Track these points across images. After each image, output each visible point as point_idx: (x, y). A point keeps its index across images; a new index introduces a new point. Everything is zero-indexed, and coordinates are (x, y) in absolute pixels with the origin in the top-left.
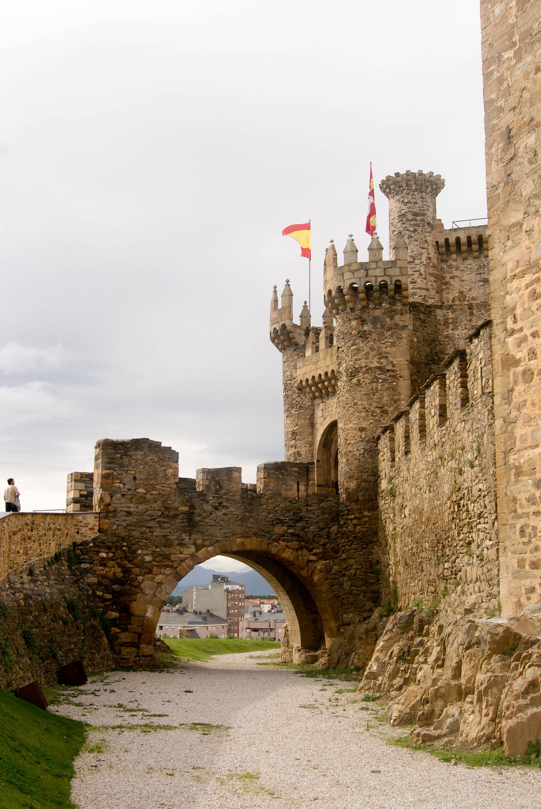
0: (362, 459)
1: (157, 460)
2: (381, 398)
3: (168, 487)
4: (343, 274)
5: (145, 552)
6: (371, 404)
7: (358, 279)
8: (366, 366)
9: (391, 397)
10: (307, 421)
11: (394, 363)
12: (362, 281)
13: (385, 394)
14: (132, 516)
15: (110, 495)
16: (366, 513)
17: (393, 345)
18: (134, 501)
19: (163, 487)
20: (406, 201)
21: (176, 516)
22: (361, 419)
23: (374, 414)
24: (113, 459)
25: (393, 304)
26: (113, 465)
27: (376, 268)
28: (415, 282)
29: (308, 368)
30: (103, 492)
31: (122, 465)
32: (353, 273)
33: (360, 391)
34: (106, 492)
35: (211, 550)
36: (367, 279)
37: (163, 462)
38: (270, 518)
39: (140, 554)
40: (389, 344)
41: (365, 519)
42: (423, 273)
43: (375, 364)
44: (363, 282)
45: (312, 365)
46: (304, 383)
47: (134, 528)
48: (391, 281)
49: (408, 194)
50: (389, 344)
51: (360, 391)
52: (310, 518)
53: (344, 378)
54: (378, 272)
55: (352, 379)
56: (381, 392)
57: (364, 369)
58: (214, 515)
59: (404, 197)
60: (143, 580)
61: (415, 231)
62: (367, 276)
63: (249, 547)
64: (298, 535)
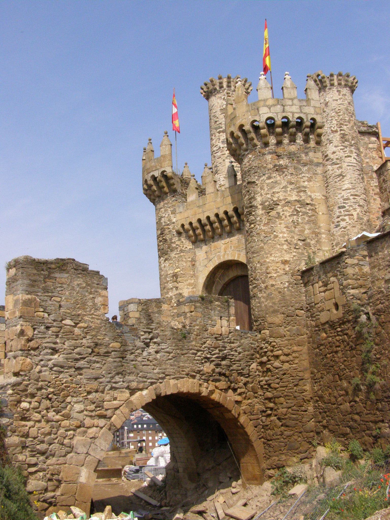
1: (84, 285)
2: (303, 231)
3: (98, 319)
4: (258, 109)
5: (75, 399)
6: (293, 237)
10: (189, 264)
11: (312, 197)
13: (307, 227)
15: (32, 327)
16: (295, 348)
17: (309, 180)
18: (60, 336)
19: (92, 318)
21: (107, 354)
22: (284, 252)
23: (297, 247)
26: (36, 289)
27: (292, 105)
29: (189, 213)
30: (25, 323)
32: (270, 108)
34: (28, 323)
35: (146, 395)
36: (284, 115)
38: (199, 356)
39: (70, 403)
40: (307, 178)
41: (294, 355)
43: (294, 198)
44: (280, 117)
45: (196, 209)
46: (187, 226)
47: (62, 370)
48: (307, 118)
50: (307, 178)
51: (280, 224)
52: (233, 355)
53: (260, 212)
54: (295, 109)
56: (302, 225)
57: (283, 202)
58: (145, 354)
59: (225, 95)
60: (74, 435)
62: (284, 111)
64: (224, 375)
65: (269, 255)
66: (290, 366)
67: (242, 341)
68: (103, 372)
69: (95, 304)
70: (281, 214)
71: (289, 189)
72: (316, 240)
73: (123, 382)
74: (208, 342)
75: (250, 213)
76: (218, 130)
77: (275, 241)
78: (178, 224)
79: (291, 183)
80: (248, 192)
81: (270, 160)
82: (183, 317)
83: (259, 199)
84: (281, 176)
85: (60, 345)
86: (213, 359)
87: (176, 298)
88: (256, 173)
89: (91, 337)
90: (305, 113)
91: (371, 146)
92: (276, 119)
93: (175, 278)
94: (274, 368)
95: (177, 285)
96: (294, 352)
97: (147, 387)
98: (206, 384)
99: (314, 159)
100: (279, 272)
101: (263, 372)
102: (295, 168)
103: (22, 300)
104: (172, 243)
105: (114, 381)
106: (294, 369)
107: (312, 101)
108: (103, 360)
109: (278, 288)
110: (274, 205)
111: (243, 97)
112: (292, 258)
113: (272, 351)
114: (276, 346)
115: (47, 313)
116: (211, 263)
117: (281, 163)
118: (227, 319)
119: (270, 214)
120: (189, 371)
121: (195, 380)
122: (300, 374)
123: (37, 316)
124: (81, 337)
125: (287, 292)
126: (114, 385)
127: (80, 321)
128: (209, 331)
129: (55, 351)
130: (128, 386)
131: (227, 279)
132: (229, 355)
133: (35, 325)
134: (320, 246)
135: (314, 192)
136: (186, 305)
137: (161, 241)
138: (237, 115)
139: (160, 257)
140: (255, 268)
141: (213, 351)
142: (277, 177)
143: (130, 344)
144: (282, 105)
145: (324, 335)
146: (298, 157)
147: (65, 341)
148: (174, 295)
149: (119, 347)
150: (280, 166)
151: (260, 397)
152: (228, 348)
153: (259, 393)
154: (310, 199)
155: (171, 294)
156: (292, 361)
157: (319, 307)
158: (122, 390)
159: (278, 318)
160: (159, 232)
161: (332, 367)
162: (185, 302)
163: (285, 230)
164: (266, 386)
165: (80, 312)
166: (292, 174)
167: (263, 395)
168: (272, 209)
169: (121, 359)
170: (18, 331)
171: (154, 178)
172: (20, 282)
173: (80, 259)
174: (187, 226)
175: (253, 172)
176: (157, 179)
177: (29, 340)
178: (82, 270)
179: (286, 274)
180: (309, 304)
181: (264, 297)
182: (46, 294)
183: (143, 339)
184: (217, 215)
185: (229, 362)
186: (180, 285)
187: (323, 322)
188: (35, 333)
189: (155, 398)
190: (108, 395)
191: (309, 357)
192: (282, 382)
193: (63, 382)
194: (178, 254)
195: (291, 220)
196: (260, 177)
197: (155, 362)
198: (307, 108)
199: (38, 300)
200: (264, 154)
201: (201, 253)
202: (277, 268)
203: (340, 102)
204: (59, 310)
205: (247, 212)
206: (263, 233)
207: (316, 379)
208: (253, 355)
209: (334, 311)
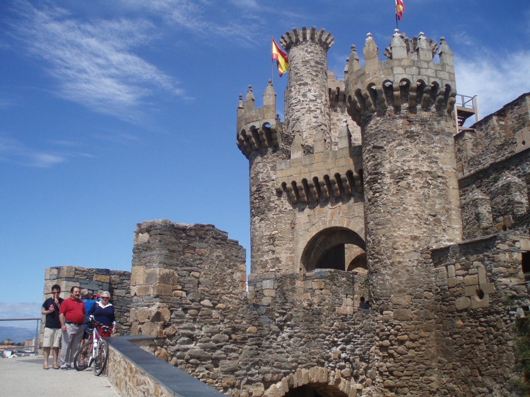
0: (416, 272)
1: (223, 258)
2: (433, 206)
3: (236, 299)
4: (392, 68)
6: (423, 211)
7: (410, 76)
9: (443, 205)
10: (288, 226)
12: (414, 79)
13: (438, 201)
14: (194, 342)
15: (169, 309)
16: (423, 333)
17: (441, 151)
18: (198, 320)
19: (231, 297)
20: (309, 50)
24: (174, 252)
26: (174, 261)
27: (428, 68)
28: (317, 117)
31: (185, 264)
33: (411, 196)
34: (165, 304)
36: (420, 77)
37: (230, 262)
40: (438, 149)
41: (421, 341)
42: (323, 111)
43: (425, 169)
46: (289, 185)
48: (442, 84)
49: (311, 45)
50: (438, 149)
51: (411, 196)
52: (356, 337)
53: (387, 180)
54: (430, 72)
55: (399, 182)
56: (432, 199)
57: (414, 173)
58: (279, 339)
59: (307, 47)
62: (419, 74)
63: (314, 380)
65: (397, 229)
66: (416, 353)
67: (364, 321)
68: (240, 363)
69: (233, 280)
70: (412, 185)
71: (420, 159)
72: (446, 216)
73: (259, 373)
74: (335, 323)
75: (375, 181)
76: (299, 83)
77: (404, 214)
78: (278, 182)
79: (423, 152)
80: (374, 157)
81: (401, 125)
82: (309, 294)
83: (387, 166)
84: (413, 144)
85: (197, 331)
86: (339, 343)
87: (272, 262)
88: (385, 137)
89: (229, 320)
90: (440, 79)
92: (411, 81)
93: (272, 241)
94: (398, 353)
95: (274, 249)
96: (421, 337)
97: (280, 378)
98: (333, 372)
99: (446, 128)
100: (407, 249)
101: (384, 357)
102: (428, 137)
103: (159, 275)
104: (270, 202)
105: (249, 372)
106: (421, 357)
107: (447, 66)
108: (240, 348)
109: (406, 266)
110: (405, 174)
111: (375, 53)
112: (422, 234)
113: (396, 335)
114: (401, 330)
115: (185, 291)
116: (314, 228)
117: (412, 129)
118: (352, 297)
119: (399, 184)
120: (319, 358)
121: (324, 368)
122: (428, 362)
123: (176, 295)
124: (219, 321)
125: (416, 271)
126: (250, 378)
127: (218, 301)
128: (336, 311)
129: (192, 339)
130: (264, 378)
132: (353, 337)
133: (173, 307)
134: (450, 223)
135: (446, 164)
136: (315, 280)
137: (256, 199)
138: (367, 73)
139: (253, 216)
140: (379, 242)
141: (339, 333)
142: (408, 144)
143: (266, 328)
144: (418, 67)
145: (460, 322)
146: (430, 125)
147: (202, 326)
148: (270, 259)
149: (255, 332)
150: (412, 132)
151: (379, 385)
152: (352, 330)
153: (377, 380)
154: (441, 171)
155: (266, 258)
156: (418, 347)
157: (455, 292)
158: (258, 383)
159: (405, 299)
160: (254, 189)
161: (471, 359)
162: (313, 277)
163: (415, 203)
164: (387, 373)
165: (218, 290)
166: (424, 143)
167: (382, 383)
168: (402, 179)
169: (257, 347)
170: (153, 314)
171: (254, 130)
172: (156, 252)
173: (219, 227)
174: (289, 185)
175: (381, 135)
176: (258, 131)
177: (165, 326)
178: (221, 239)
179: (415, 251)
180: (439, 287)
181: (389, 275)
182: (185, 268)
183: (278, 322)
185: (352, 346)
186: (277, 249)
187: (459, 309)
188: (172, 316)
189: (287, 390)
190: (244, 390)
191: (437, 344)
192: (407, 370)
193: (199, 377)
194: (277, 214)
195: (422, 193)
196: (389, 142)
197: (289, 349)
198: (442, 73)
199: (176, 275)
200: (394, 118)
201: (302, 217)
202: (405, 244)
204: (198, 287)
205: (370, 179)
206: (391, 204)
207: (446, 369)
208: (372, 337)
209: (477, 299)
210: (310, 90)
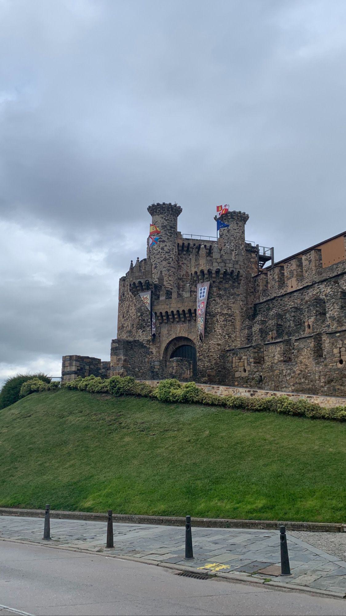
8: (220, 313)
17: (234, 303)
25: (234, 282)
43: (225, 312)
54: (230, 265)
61: (171, 236)
91: (252, 260)
102: (228, 297)
131: (177, 346)
184: (178, 311)
203: (237, 231)
210: (166, 246)
